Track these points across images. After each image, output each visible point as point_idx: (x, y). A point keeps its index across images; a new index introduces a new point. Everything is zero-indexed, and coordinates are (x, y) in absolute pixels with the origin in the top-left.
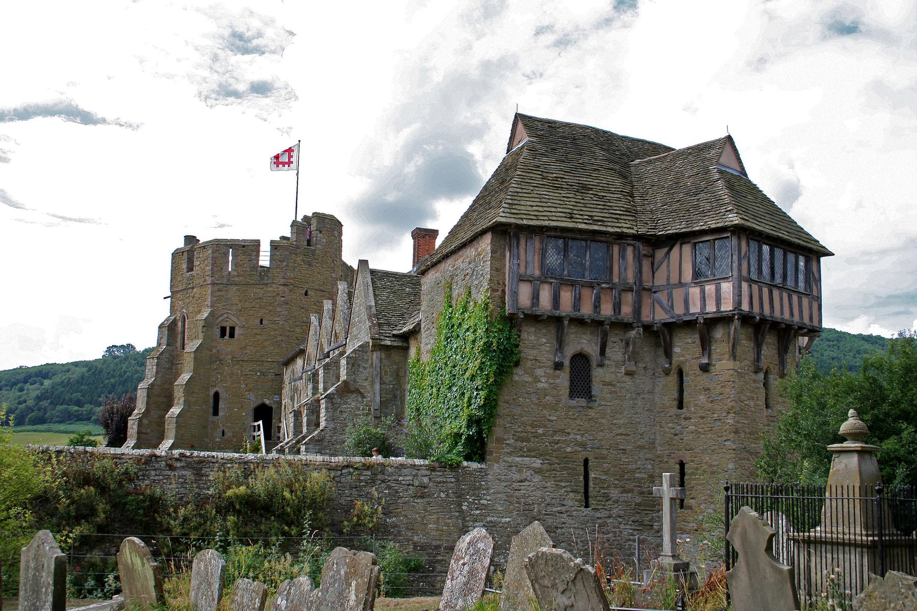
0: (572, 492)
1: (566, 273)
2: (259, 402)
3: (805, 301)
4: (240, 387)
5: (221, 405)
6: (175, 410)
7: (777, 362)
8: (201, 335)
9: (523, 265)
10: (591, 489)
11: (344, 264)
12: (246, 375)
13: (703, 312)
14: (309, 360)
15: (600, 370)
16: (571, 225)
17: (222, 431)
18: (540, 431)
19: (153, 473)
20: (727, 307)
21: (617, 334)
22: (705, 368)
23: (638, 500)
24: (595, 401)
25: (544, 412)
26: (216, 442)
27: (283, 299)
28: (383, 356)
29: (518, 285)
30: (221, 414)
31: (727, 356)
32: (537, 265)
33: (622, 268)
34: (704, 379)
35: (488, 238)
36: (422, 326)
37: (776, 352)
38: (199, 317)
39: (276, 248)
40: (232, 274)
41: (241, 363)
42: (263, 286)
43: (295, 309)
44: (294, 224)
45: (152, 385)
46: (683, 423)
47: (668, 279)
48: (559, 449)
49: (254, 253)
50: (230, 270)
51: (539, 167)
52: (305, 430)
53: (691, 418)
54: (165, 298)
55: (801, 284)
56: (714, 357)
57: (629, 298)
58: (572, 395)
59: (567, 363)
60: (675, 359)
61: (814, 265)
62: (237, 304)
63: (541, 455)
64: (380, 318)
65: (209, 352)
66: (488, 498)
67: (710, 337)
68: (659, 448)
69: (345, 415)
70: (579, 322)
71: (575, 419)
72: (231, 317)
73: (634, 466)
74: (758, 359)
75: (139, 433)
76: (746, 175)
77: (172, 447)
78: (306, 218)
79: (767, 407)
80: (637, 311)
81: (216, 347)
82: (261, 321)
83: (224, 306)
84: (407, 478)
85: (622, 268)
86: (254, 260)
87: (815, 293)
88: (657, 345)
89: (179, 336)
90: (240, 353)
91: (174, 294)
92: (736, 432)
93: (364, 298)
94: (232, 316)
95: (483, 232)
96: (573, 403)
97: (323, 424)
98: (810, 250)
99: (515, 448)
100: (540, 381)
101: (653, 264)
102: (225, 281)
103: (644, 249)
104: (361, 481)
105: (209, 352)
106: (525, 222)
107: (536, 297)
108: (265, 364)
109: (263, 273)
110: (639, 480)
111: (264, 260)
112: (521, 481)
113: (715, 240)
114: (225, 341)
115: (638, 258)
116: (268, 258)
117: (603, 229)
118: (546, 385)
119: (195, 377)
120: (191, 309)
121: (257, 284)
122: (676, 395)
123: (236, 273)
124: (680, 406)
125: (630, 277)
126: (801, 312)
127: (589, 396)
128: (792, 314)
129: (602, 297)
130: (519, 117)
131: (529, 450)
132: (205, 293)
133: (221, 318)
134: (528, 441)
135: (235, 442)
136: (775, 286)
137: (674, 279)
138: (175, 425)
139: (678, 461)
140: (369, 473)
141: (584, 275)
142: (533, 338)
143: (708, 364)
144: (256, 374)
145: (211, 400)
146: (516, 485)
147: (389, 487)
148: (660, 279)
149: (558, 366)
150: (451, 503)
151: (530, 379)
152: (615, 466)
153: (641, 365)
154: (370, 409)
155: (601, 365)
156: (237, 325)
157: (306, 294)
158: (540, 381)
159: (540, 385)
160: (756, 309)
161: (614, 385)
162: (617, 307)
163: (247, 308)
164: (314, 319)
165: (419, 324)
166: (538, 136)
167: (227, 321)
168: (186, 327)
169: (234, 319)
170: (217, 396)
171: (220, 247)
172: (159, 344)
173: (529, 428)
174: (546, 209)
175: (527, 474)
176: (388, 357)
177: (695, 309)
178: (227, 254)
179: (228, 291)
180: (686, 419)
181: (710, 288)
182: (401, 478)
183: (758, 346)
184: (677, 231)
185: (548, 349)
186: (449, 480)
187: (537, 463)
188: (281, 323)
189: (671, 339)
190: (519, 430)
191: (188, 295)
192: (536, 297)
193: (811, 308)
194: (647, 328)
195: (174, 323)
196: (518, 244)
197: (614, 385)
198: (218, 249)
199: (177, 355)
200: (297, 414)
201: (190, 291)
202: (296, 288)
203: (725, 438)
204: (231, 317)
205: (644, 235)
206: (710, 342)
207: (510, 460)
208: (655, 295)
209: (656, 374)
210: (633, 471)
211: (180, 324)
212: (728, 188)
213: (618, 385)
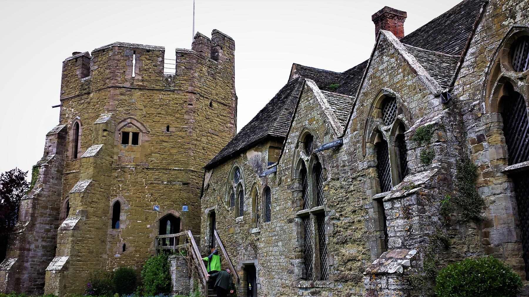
2: (166, 213)
4: (144, 197)
5: (123, 216)
6: (71, 222)
17: (122, 245)
26: (116, 259)
27: (191, 106)
30: (122, 226)
38: (98, 121)
39: (183, 56)
40: (136, 78)
41: (145, 170)
42: (169, 93)
43: (201, 118)
45: (39, 195)
49: (160, 59)
50: (134, 75)
54: (53, 107)
65: (111, 159)
72: (135, 122)
81: (117, 153)
83: (127, 110)
86: (159, 65)
90: (145, 161)
102: (127, 85)
105: (108, 158)
108: (173, 173)
109: (169, 79)
114: (127, 147)
119: (94, 184)
121: (162, 90)
123: (140, 78)
132: (104, 97)
135: (137, 258)
138: (71, 239)
144: (163, 182)
156: (140, 130)
157: (211, 105)
163: (153, 114)
167: (130, 127)
168: (80, 134)
169: (139, 125)
170: (117, 206)
172: (47, 153)
178: (128, 58)
179: (131, 95)
188: (189, 131)
191: (82, 101)
195: (65, 131)
198: (121, 51)
199: (67, 165)
201: (83, 97)
202: (202, 98)
204: (135, 122)
211: (71, 133)
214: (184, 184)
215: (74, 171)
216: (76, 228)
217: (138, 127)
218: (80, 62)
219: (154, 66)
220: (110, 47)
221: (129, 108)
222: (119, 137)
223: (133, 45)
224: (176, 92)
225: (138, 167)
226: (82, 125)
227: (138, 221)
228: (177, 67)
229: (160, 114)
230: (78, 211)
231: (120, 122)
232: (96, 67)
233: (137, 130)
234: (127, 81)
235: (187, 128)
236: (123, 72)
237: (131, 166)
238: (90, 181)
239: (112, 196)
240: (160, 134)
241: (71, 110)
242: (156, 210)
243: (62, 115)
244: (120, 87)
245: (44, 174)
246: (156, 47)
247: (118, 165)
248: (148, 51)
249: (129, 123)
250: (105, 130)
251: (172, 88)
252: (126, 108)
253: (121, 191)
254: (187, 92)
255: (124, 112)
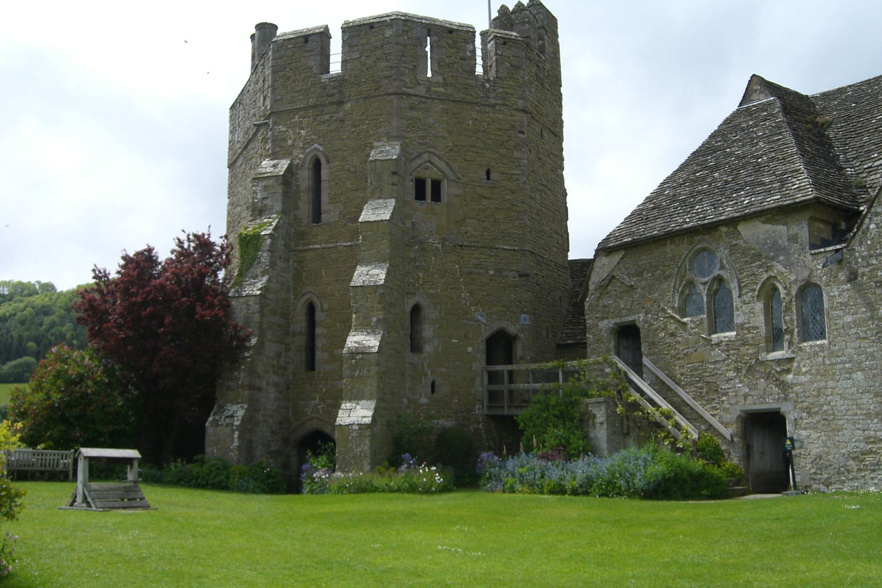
2: (496, 326)
5: (428, 331)
12: (470, 273)
17: (430, 383)
27: (522, 135)
30: (428, 348)
39: (505, 44)
41: (459, 250)
42: (487, 109)
62: (445, 138)
65: (402, 225)
72: (435, 160)
82: (488, 173)
83: (421, 137)
94: (437, 159)
102: (421, 91)
109: (487, 85)
114: (425, 205)
121: (477, 104)
156: (445, 175)
167: (427, 168)
169: (442, 165)
191: (327, 117)
198: (407, 28)
204: (435, 160)
214: (521, 276)
215: (318, 246)
217: (440, 170)
219: (461, 59)
220: (386, 21)
221: (425, 135)
224: (498, 108)
225: (447, 243)
226: (328, 162)
227: (453, 341)
229: (475, 147)
230: (374, 319)
231: (414, 159)
233: (438, 175)
234: (419, 84)
235: (519, 175)
236: (411, 67)
237: (434, 241)
239: (407, 293)
240: (477, 184)
241: (299, 133)
242: (478, 321)
244: (410, 95)
245: (269, 250)
246: (461, 26)
247: (414, 238)
249: (426, 162)
250: (395, 173)
251: (492, 101)
252: (421, 133)
253: (420, 284)
254: (517, 110)
255: (418, 140)
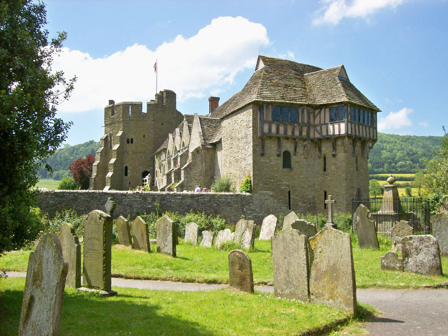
0: (285, 203)
1: (281, 120)
3: (371, 129)
6: (110, 174)
7: (361, 153)
8: (119, 142)
9: (265, 117)
10: (291, 202)
11: (177, 111)
13: (334, 135)
14: (169, 153)
15: (294, 157)
16: (283, 101)
18: (272, 181)
19: (128, 200)
20: (343, 132)
21: (301, 143)
22: (334, 156)
23: (309, 206)
24: (292, 169)
25: (274, 173)
28: (206, 152)
29: (263, 125)
30: (128, 175)
31: (343, 151)
32: (270, 117)
33: (303, 117)
34: (333, 160)
35: (251, 106)
36: (222, 139)
37: (360, 149)
44: (156, 95)
45: (99, 164)
46: (326, 177)
47: (320, 122)
48: (279, 188)
49: (140, 107)
51: (269, 78)
52: (173, 182)
53: (328, 175)
55: (370, 123)
56: (337, 151)
57: (305, 129)
58: (284, 167)
59: (282, 154)
60: (323, 152)
61: (375, 115)
63: (273, 190)
64: (205, 136)
66: (253, 206)
67: (336, 144)
68: (316, 186)
69: (191, 176)
70: (287, 139)
71: (285, 176)
73: (307, 194)
74: (354, 152)
75: (94, 184)
76: (349, 80)
77: (109, 189)
78: (161, 92)
79: (357, 170)
80: (308, 133)
84: (223, 200)
85: (303, 117)
87: (375, 126)
88: (316, 147)
89: (109, 143)
91: (106, 125)
92: (346, 179)
93: (197, 129)
95: (249, 104)
96: (285, 170)
97: (183, 179)
98: (373, 110)
99: (263, 187)
100: (272, 162)
101: (314, 115)
103: (311, 110)
104: (206, 201)
106: (265, 100)
107: (270, 129)
110: (309, 198)
111: (145, 110)
112: (266, 200)
113: (338, 107)
115: (309, 114)
116: (146, 109)
117: (295, 102)
118: (274, 163)
120: (114, 132)
122: (323, 166)
123: (132, 116)
124: (325, 170)
125: (306, 121)
126: (370, 133)
127: (291, 167)
128: (366, 135)
129: (295, 129)
130: (260, 57)
131: (268, 188)
133: (127, 135)
134: (268, 185)
136: (360, 124)
137: (322, 121)
139: (324, 191)
140: (208, 198)
141: (288, 120)
142: (269, 145)
143: (335, 154)
145: (124, 170)
146: (263, 201)
147: (216, 203)
148: (317, 122)
149: (279, 155)
150: (240, 208)
151: (268, 161)
152: (300, 193)
153: (310, 155)
154: (201, 173)
155: (295, 154)
157: (162, 124)
158: (272, 162)
159: (272, 163)
160: (354, 133)
161: (300, 163)
162: (301, 133)
164: (170, 136)
165: (221, 139)
166: (268, 65)
168: (112, 139)
170: (126, 168)
171: (126, 106)
173: (268, 180)
174: (273, 95)
175: (267, 197)
176: (208, 152)
177: (331, 133)
180: (327, 175)
181: (336, 126)
182: (220, 200)
183: (354, 146)
184: (324, 103)
185: (275, 149)
186: (238, 200)
187: (271, 193)
189: (321, 145)
190: (264, 180)
192: (270, 129)
193: (373, 132)
194: (312, 140)
195: (107, 137)
196: (263, 109)
197: (300, 163)
200: (169, 175)
203: (342, 182)
205: (311, 104)
206: (336, 146)
207: (261, 192)
208: (315, 128)
209: (316, 158)
210: (307, 195)
211: (109, 138)
212: (343, 87)
213: (301, 162)
216: (112, 176)
218: (110, 109)
222: (126, 141)
223: (130, 102)
228: (147, 110)
232: (116, 112)
238: (116, 159)
243: (106, 131)
248: (136, 104)
